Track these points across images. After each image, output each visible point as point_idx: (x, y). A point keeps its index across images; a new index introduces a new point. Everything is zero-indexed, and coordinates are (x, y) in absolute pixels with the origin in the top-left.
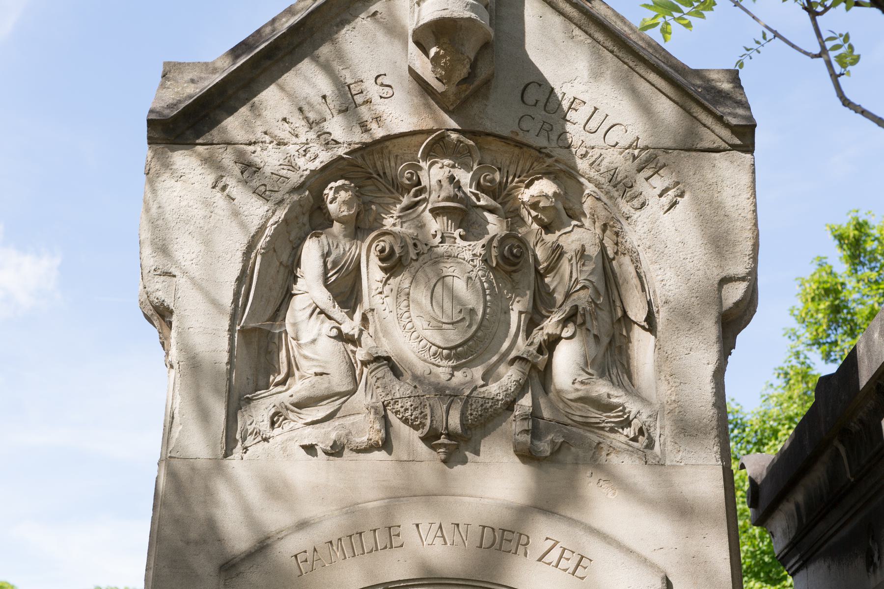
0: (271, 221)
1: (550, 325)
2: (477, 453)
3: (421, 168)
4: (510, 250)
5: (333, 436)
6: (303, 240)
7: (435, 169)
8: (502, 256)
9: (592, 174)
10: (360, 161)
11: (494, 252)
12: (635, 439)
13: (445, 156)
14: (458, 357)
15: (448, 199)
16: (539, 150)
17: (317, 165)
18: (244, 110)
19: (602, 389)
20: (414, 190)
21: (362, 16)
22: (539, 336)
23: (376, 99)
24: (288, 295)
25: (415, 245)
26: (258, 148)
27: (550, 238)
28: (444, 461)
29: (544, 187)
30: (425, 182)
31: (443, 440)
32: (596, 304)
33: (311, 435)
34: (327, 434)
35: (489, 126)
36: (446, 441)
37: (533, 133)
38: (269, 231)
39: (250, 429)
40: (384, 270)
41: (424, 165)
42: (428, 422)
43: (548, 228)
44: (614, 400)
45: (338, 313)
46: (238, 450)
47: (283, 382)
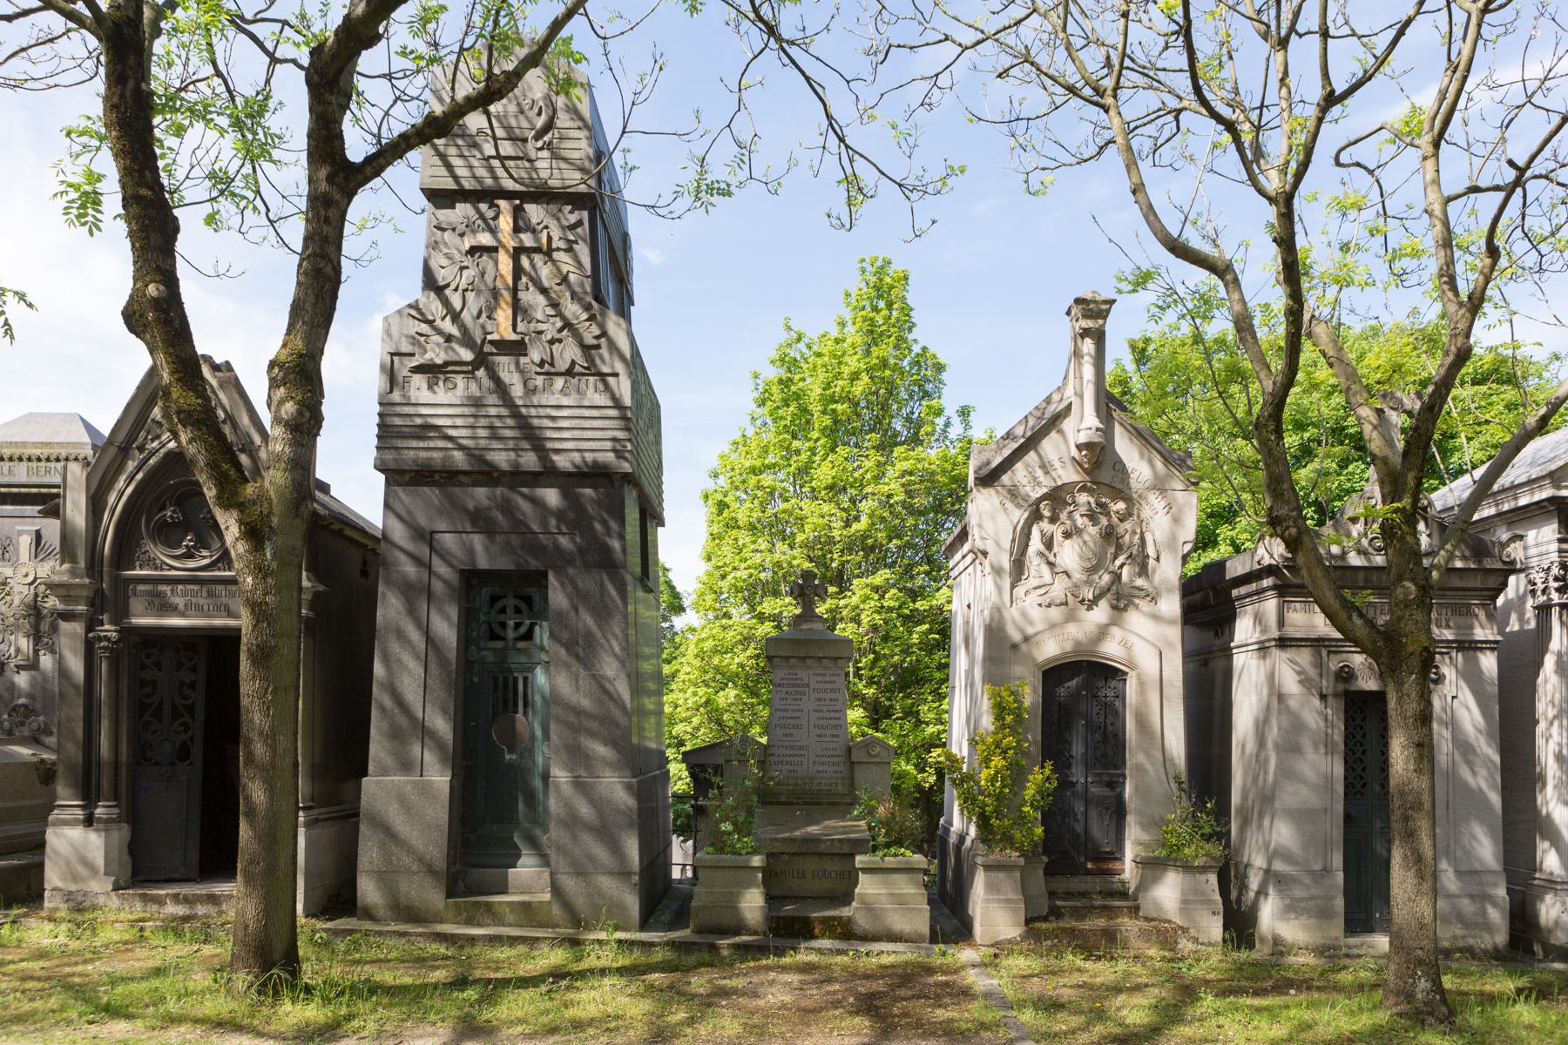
17: (1038, 495)
19: (1140, 582)
22: (1118, 563)
29: (1121, 506)
35: (1101, 480)
38: (1022, 522)
43: (1121, 521)
45: (1047, 553)
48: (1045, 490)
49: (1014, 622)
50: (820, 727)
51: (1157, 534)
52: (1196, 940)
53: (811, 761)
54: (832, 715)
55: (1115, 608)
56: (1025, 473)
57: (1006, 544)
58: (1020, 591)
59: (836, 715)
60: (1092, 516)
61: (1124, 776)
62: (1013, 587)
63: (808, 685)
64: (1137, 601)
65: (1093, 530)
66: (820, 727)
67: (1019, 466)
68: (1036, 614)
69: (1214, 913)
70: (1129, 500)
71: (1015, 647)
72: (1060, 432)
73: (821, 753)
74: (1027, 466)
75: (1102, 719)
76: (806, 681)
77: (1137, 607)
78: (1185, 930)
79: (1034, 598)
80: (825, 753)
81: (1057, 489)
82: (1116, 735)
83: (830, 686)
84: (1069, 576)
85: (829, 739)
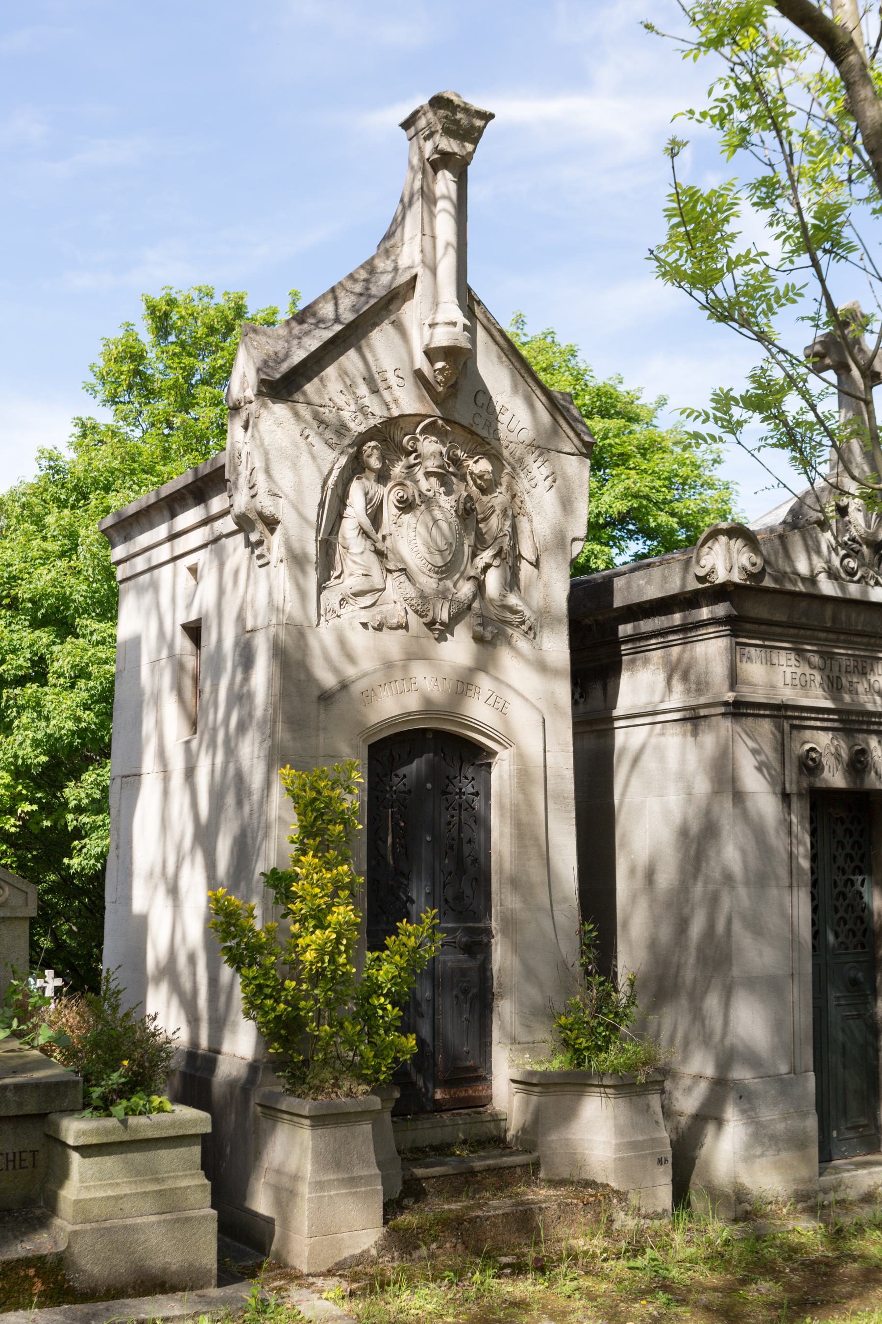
0: (336, 466)
1: (486, 556)
2: (452, 635)
3: (418, 440)
5: (379, 618)
9: (511, 460)
13: (433, 434)
14: (442, 573)
16: (483, 439)
17: (362, 429)
18: (316, 380)
21: (386, 321)
23: (395, 387)
24: (340, 517)
26: (326, 410)
27: (485, 499)
28: (436, 639)
29: (483, 466)
31: (437, 626)
33: (365, 616)
34: (374, 616)
35: (457, 418)
37: (481, 426)
38: (336, 473)
41: (421, 438)
42: (431, 614)
47: (339, 577)
48: (373, 422)
49: (327, 659)
51: (536, 519)
52: (637, 1212)
55: (479, 639)
56: (340, 387)
57: (312, 514)
58: (331, 597)
60: (443, 478)
61: (488, 932)
62: (320, 589)
64: (510, 631)
65: (447, 502)
67: (331, 371)
68: (360, 640)
69: (660, 1162)
70: (495, 458)
71: (326, 698)
72: (399, 326)
74: (344, 373)
75: (455, 831)
77: (509, 641)
78: (622, 1196)
79: (354, 613)
81: (391, 422)
82: (476, 861)
84: (410, 579)
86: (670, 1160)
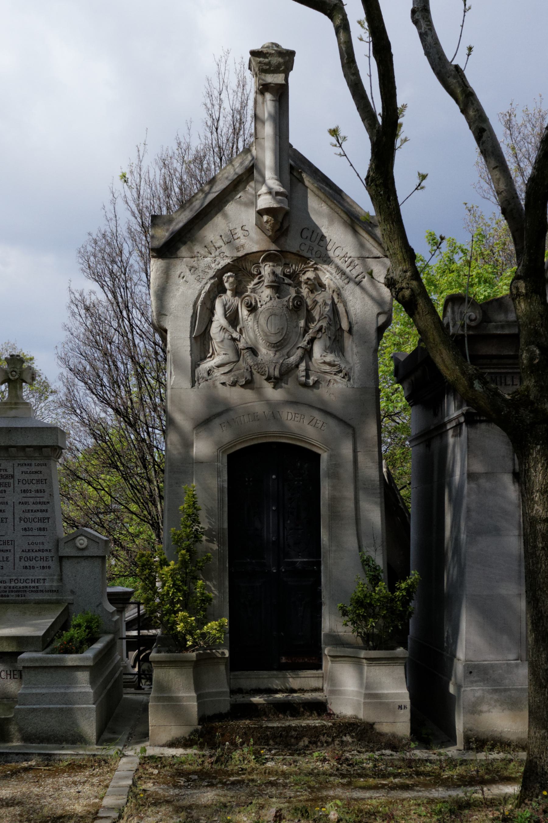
0: (203, 292)
4: (297, 303)
6: (215, 298)
7: (266, 268)
8: (293, 304)
10: (236, 264)
11: (291, 304)
12: (343, 378)
13: (270, 261)
14: (278, 347)
15: (272, 282)
17: (220, 267)
20: (258, 276)
24: (211, 322)
25: (260, 301)
28: (274, 388)
30: (263, 273)
31: (272, 380)
32: (330, 324)
36: (274, 381)
38: (202, 296)
39: (200, 376)
40: (248, 311)
42: (267, 373)
44: (336, 363)
45: (230, 329)
46: (196, 384)
47: (211, 357)
50: (26, 520)
53: (17, 556)
54: (39, 507)
59: (44, 507)
63: (13, 476)
66: (26, 520)
73: (27, 547)
76: (10, 472)
80: (32, 547)
81: (239, 259)
83: (35, 477)
85: (36, 533)
86: (409, 707)
